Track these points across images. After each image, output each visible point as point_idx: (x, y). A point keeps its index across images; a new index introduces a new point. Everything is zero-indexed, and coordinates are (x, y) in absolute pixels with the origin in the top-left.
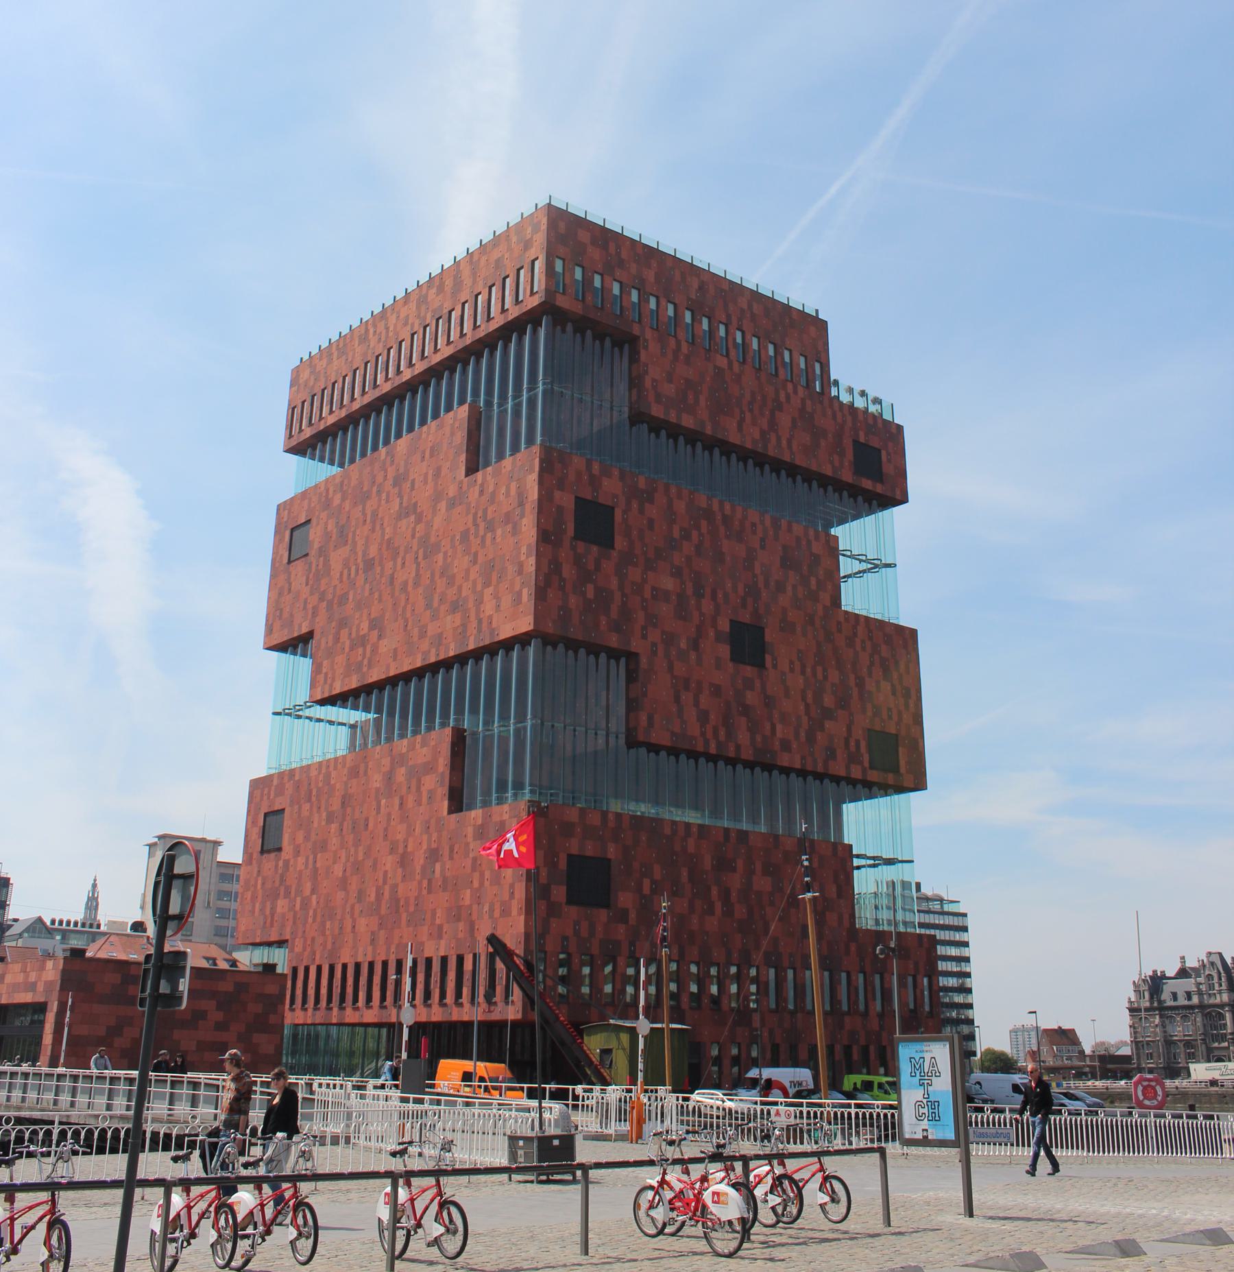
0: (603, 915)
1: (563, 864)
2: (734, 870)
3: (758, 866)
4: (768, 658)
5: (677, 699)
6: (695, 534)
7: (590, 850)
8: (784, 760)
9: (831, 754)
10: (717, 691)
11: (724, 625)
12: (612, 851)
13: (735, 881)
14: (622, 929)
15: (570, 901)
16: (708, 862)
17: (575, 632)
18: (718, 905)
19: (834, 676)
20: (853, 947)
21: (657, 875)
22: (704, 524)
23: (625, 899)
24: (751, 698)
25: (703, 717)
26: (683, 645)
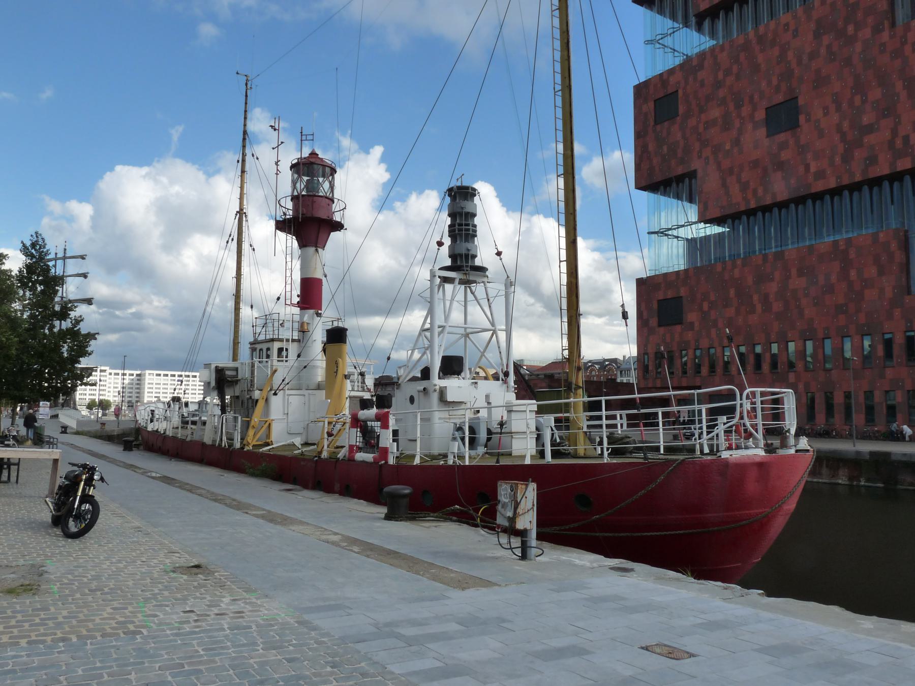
0: (678, 328)
1: (655, 306)
2: (772, 280)
3: (794, 271)
4: (802, 118)
5: (724, 185)
6: (735, 68)
7: (670, 294)
8: (819, 186)
9: (872, 160)
10: (755, 164)
11: (761, 115)
12: (683, 292)
13: (773, 288)
14: (690, 335)
15: (660, 325)
16: (750, 280)
17: (659, 177)
18: (759, 308)
19: (876, 94)
20: (897, 313)
21: (712, 297)
22: (742, 56)
23: (692, 317)
24: (785, 155)
25: (744, 187)
26: (728, 147)
